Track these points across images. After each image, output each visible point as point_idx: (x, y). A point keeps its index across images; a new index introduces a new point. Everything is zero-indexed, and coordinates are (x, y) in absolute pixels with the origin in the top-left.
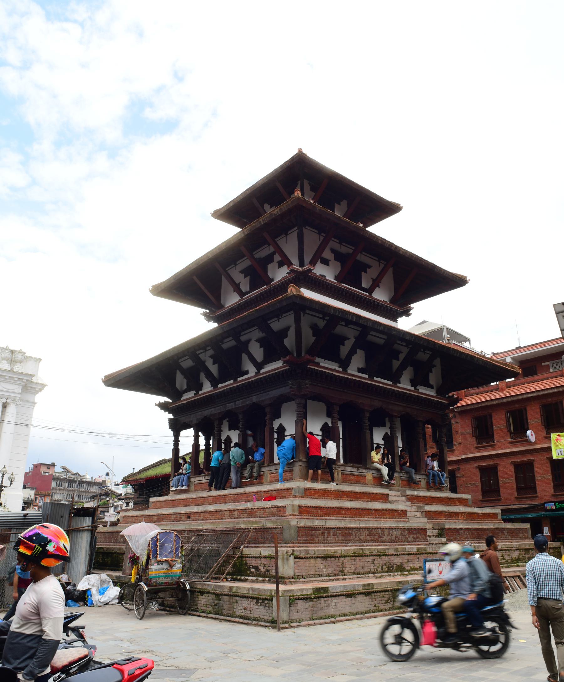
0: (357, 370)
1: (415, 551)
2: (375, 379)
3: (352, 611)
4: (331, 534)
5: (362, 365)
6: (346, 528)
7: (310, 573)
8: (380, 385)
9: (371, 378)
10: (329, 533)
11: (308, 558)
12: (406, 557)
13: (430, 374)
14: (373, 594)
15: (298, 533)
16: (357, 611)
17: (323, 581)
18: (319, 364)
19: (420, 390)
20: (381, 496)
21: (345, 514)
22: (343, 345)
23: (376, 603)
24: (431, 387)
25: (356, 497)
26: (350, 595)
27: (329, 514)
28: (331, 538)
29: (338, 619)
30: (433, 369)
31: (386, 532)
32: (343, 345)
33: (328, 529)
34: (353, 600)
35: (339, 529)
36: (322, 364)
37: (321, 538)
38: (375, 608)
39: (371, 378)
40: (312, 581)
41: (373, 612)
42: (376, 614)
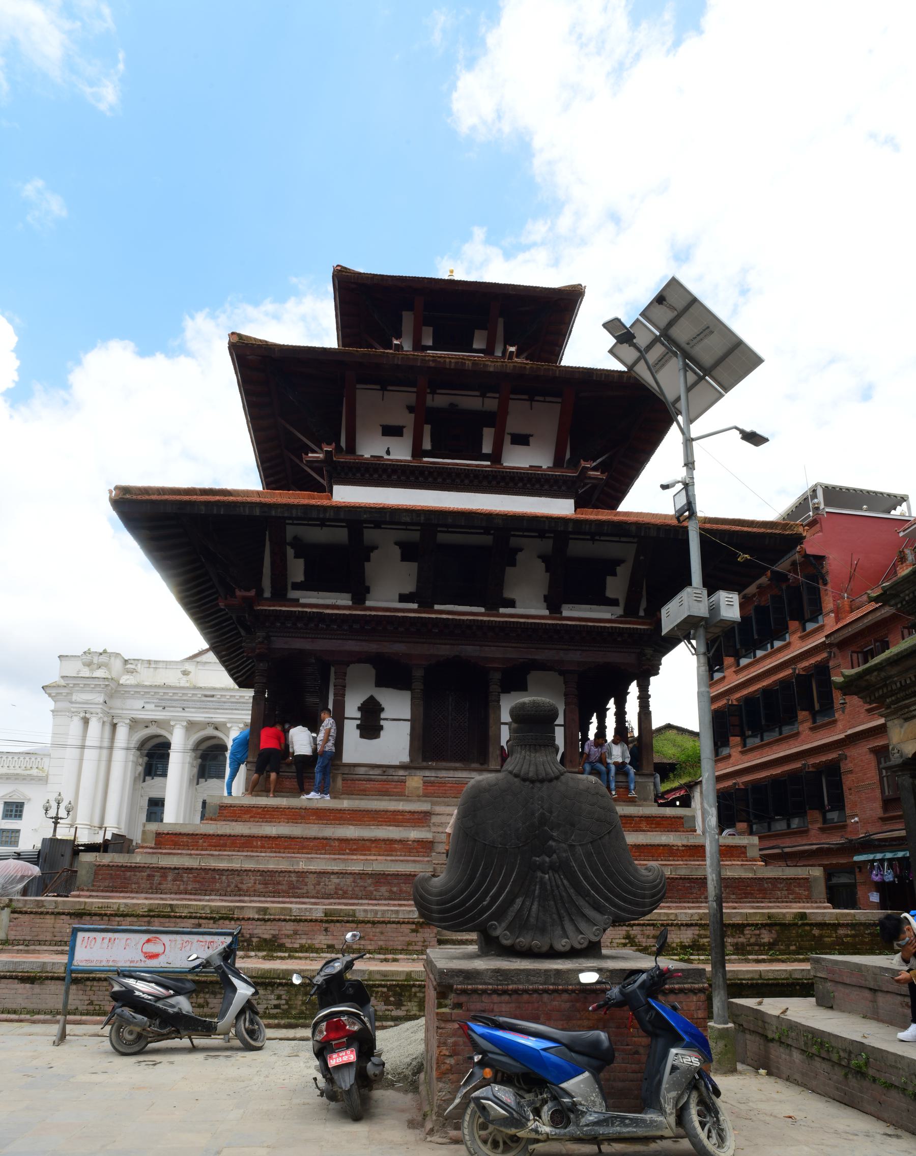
0: (397, 597)
1: (319, 915)
2: (437, 607)
3: (30, 1006)
4: (169, 878)
5: (409, 587)
6: (206, 870)
7: (41, 938)
8: (444, 616)
9: (426, 605)
10: (164, 877)
11: (42, 913)
12: (289, 928)
13: (609, 579)
14: (88, 983)
15: (96, 874)
16: (43, 1007)
17: (27, 952)
18: (298, 600)
19: (566, 613)
20: (408, 816)
21: (264, 847)
22: (369, 560)
23: (94, 998)
24: (614, 603)
25: (340, 819)
26: (29, 979)
27: (225, 845)
28: (168, 885)
29: (22, 1017)
30: (619, 569)
31: (311, 879)
32: (369, 560)
33: (164, 871)
34: (37, 988)
35: (189, 870)
36: (302, 601)
37: (145, 884)
38: (91, 1008)
39: (426, 605)
40: (38, 952)
41: (82, 1014)
42: (84, 1018)
